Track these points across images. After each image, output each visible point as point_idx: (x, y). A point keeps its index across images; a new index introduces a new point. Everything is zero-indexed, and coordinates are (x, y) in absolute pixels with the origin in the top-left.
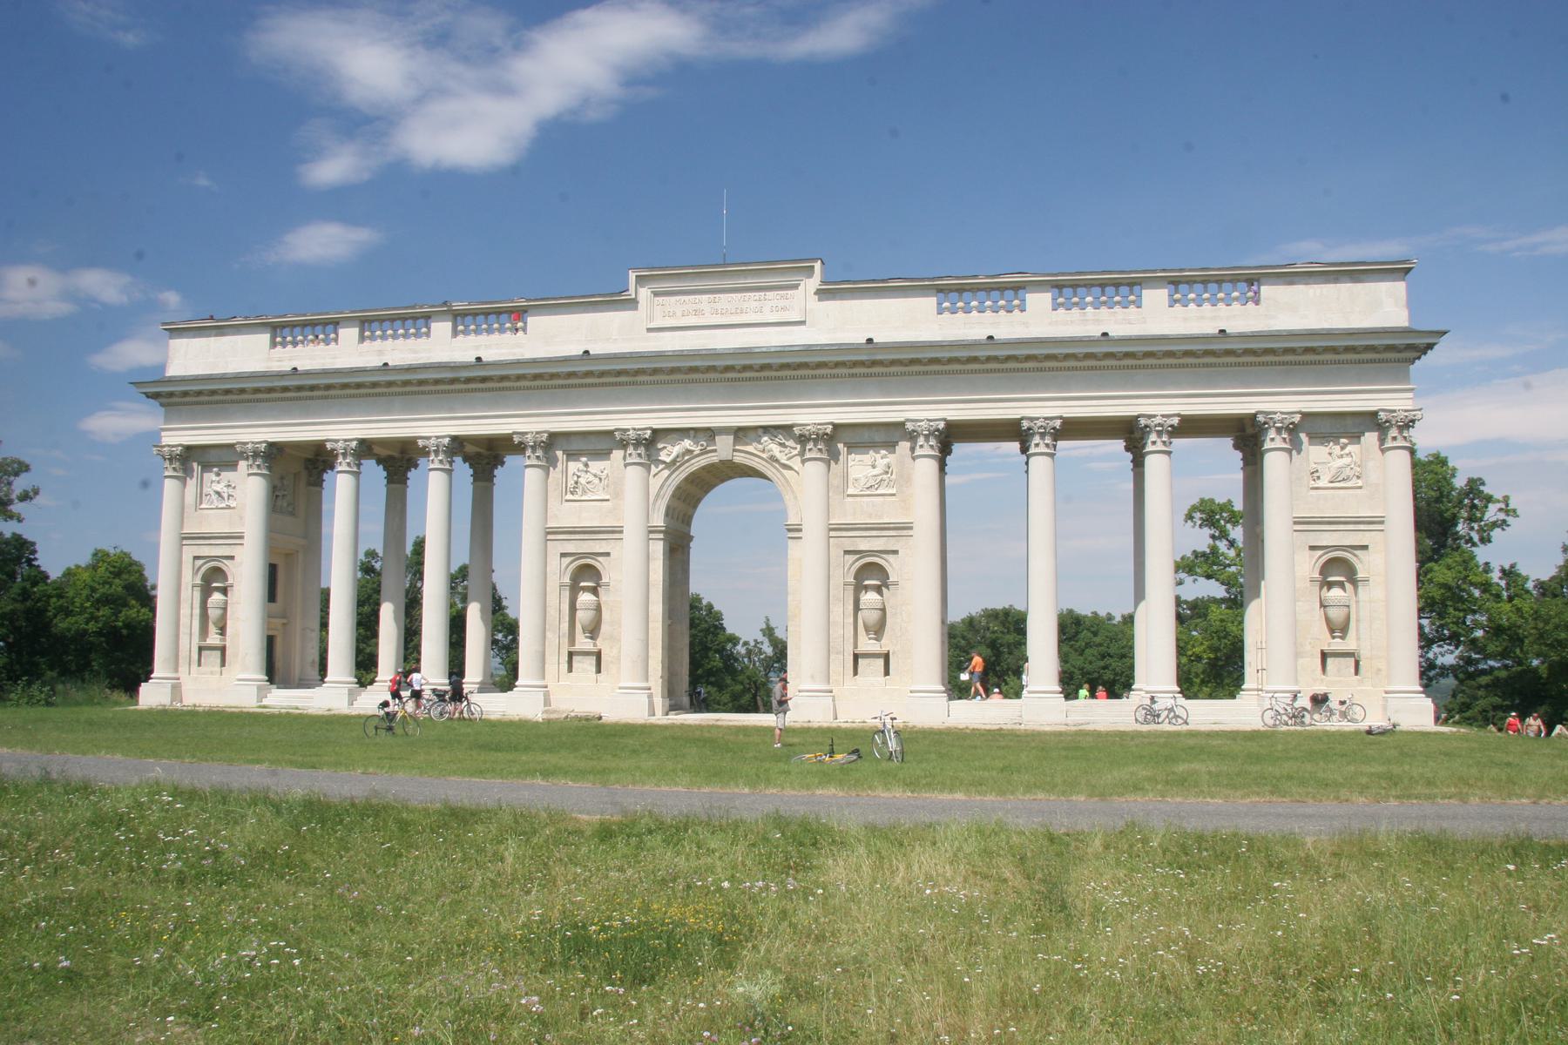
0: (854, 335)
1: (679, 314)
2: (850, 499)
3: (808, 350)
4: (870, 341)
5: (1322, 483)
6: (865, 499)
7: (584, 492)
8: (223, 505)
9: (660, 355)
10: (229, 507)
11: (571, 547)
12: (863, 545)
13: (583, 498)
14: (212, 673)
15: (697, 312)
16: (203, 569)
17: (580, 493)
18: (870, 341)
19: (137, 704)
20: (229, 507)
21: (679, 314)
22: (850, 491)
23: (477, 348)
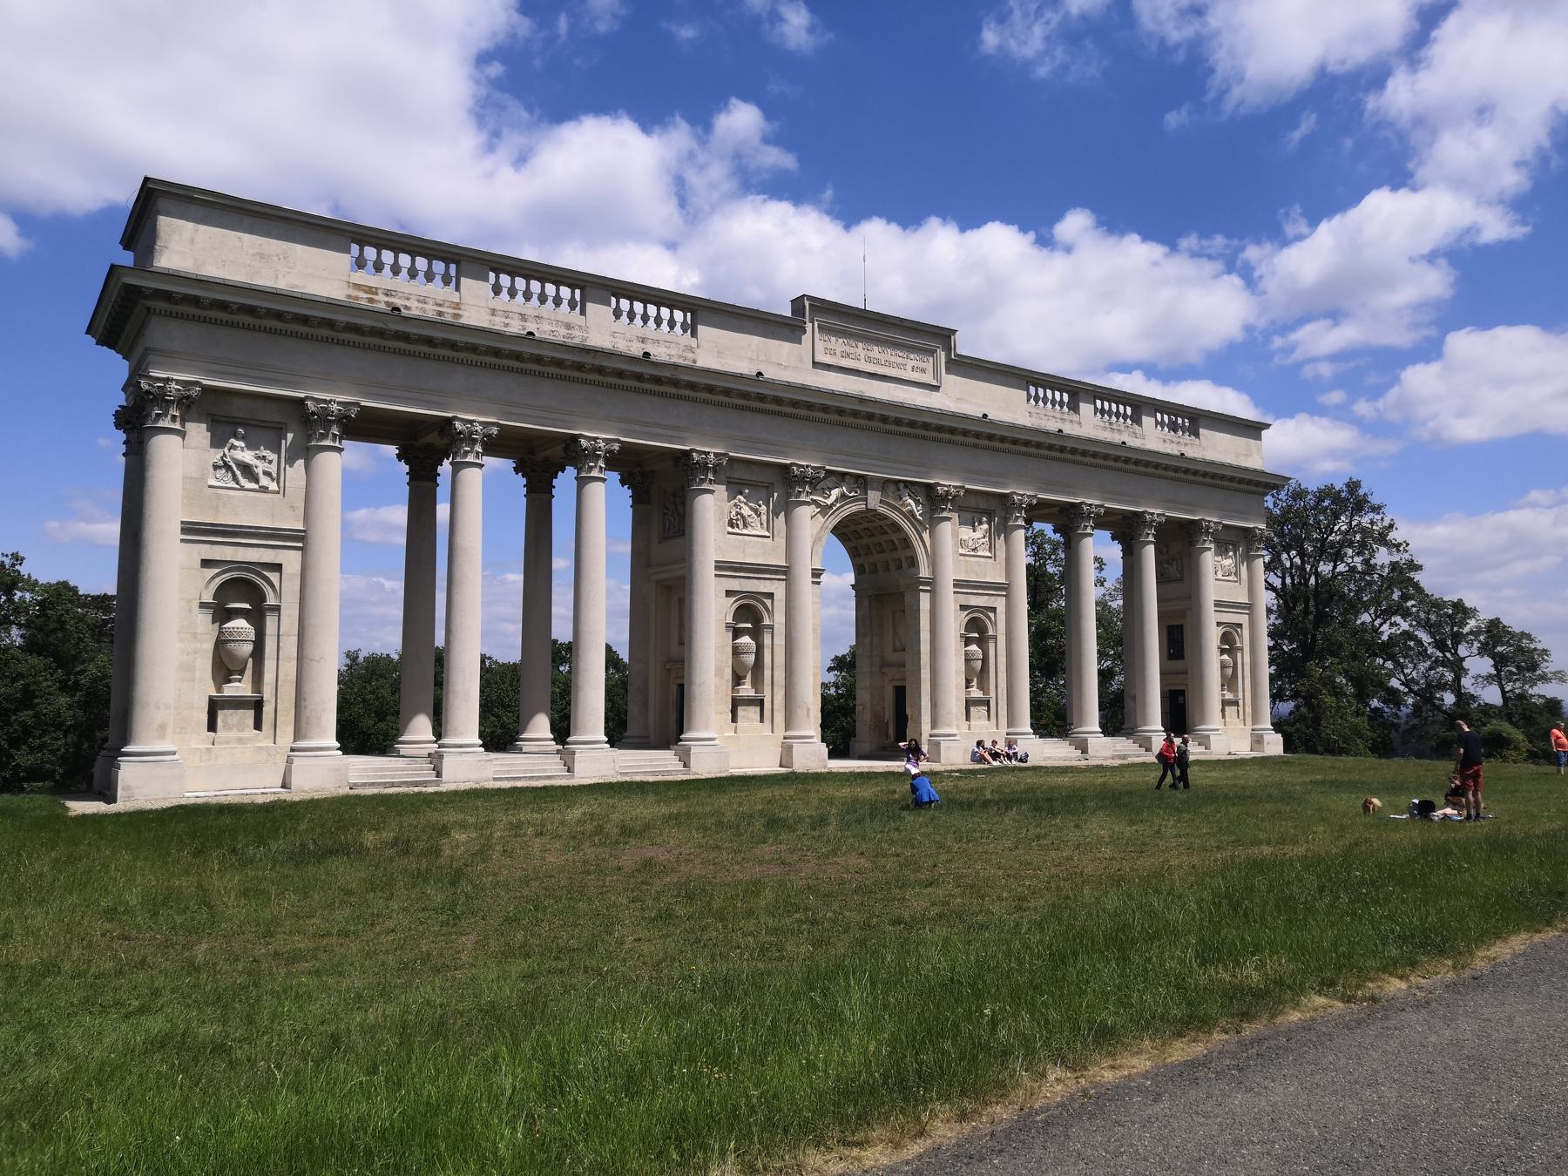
0: (973, 409)
1: (838, 354)
2: (962, 558)
3: (942, 414)
4: (985, 416)
5: (1220, 576)
6: (973, 559)
7: (745, 526)
8: (256, 486)
9: (819, 392)
10: (264, 489)
11: (735, 585)
12: (975, 601)
13: (745, 531)
14: (240, 740)
15: (869, 360)
16: (218, 581)
17: (741, 526)
18: (985, 416)
19: (110, 798)
20: (264, 489)
21: (838, 354)
22: (961, 551)
23: (643, 340)
